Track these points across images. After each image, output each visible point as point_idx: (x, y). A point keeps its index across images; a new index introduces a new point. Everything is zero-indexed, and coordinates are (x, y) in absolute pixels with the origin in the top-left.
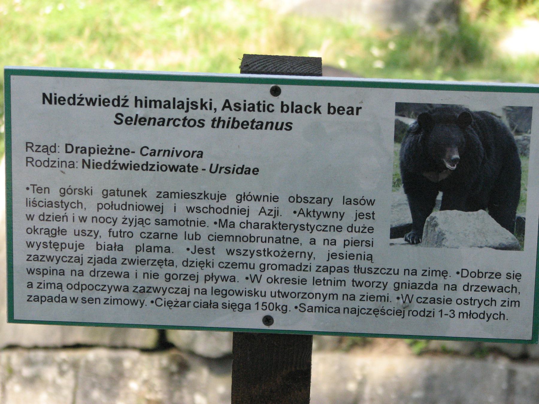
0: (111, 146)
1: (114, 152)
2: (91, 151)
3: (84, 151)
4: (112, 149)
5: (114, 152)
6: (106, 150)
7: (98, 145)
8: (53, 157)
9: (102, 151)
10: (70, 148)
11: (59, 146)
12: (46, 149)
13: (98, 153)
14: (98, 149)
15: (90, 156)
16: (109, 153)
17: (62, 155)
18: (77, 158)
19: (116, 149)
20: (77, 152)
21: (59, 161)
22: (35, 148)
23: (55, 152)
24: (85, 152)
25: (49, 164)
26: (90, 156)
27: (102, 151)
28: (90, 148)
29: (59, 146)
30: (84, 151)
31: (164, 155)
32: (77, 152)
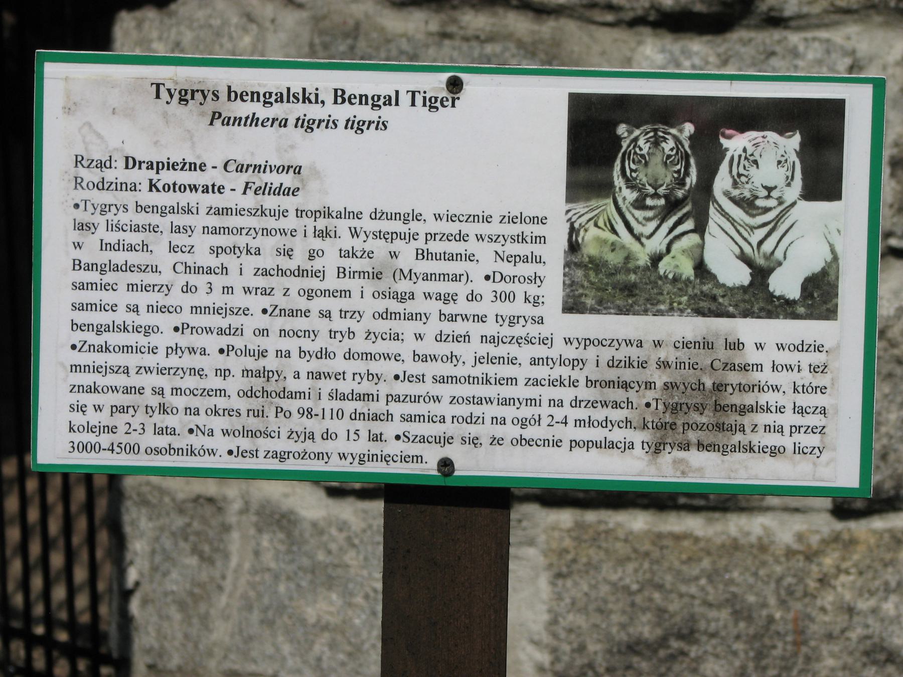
0: (184, 160)
1: (187, 166)
2: (158, 167)
3: (150, 166)
4: (185, 164)
5: (187, 166)
6: (178, 165)
7: (169, 159)
8: (109, 175)
9: (172, 166)
10: (131, 163)
11: (116, 161)
12: (101, 165)
13: (168, 169)
14: (168, 163)
15: (158, 173)
16: (182, 169)
17: (118, 173)
18: (142, 176)
19: (190, 164)
20: (140, 168)
21: (116, 183)
22: (85, 163)
23: (111, 167)
24: (152, 168)
25: (101, 186)
26: (158, 173)
27: (172, 166)
28: (158, 163)
29: (116, 161)
30: (150, 166)
31: (254, 172)
32: (140, 168)
